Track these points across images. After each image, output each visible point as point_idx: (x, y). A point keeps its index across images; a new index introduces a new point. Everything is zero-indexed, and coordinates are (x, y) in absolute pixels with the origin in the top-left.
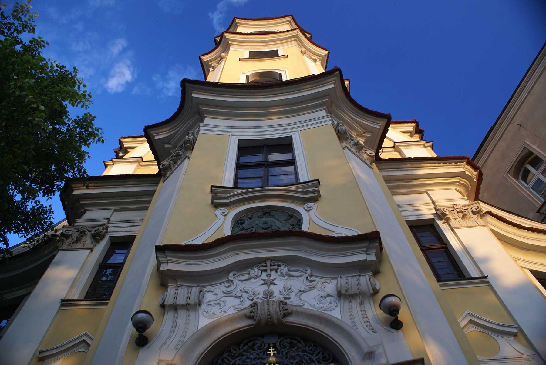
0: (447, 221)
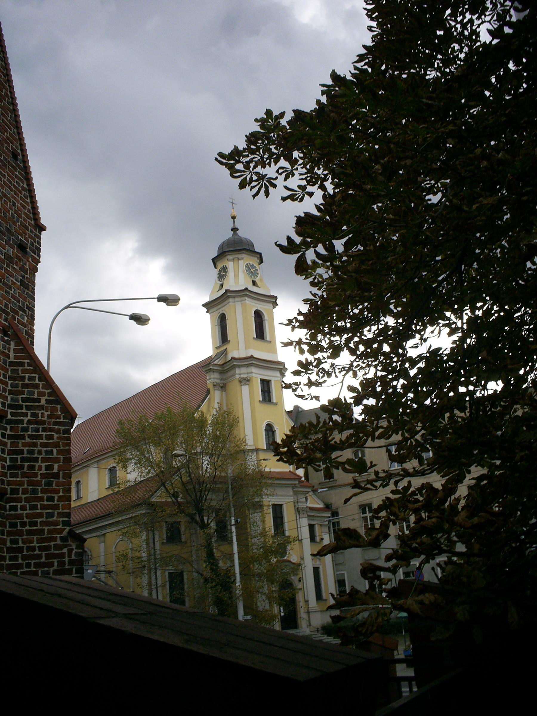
0: (299, 514)
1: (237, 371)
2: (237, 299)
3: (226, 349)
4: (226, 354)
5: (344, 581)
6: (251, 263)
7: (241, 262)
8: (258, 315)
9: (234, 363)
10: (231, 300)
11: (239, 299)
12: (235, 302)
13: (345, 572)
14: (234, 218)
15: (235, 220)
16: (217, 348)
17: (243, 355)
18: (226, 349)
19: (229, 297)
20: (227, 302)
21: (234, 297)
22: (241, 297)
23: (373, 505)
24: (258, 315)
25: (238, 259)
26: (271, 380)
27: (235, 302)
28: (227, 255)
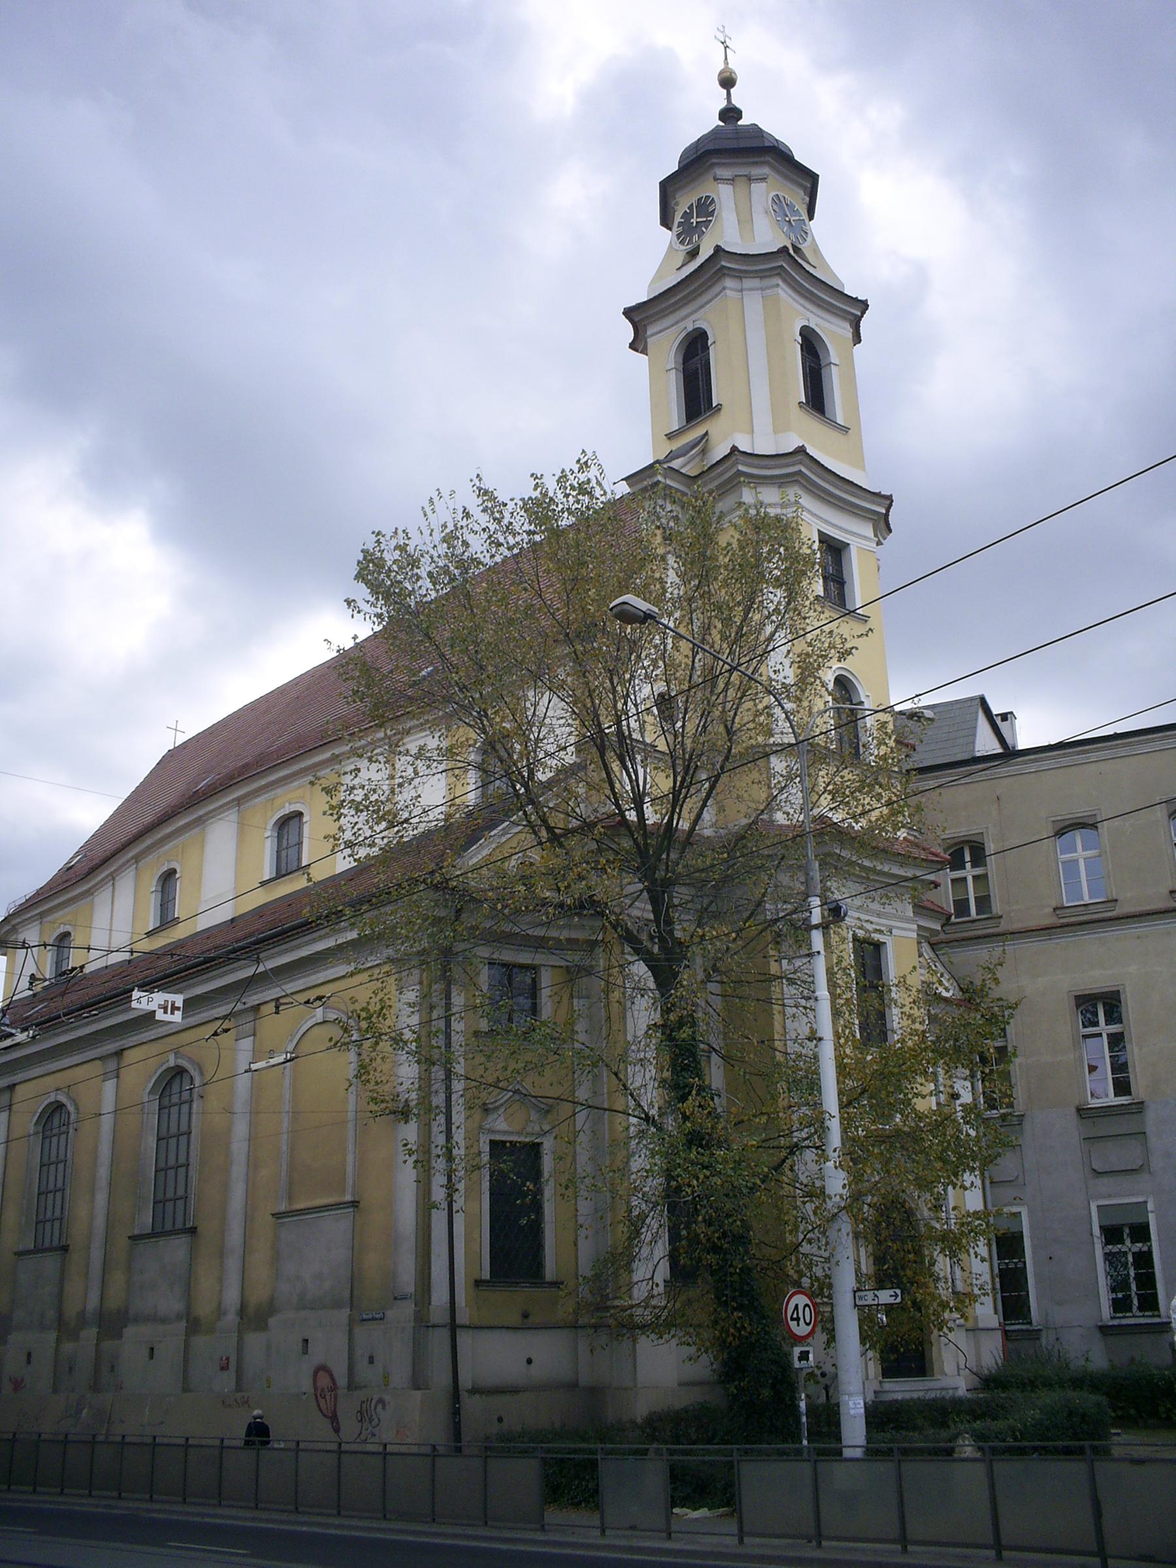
1: (748, 496)
2: (748, 283)
3: (707, 432)
4: (704, 451)
5: (1019, 1237)
6: (789, 199)
7: (758, 188)
8: (811, 345)
9: (741, 468)
10: (729, 283)
11: (756, 283)
12: (741, 290)
13: (1024, 1211)
14: (727, 82)
15: (732, 90)
16: (670, 436)
17: (765, 447)
18: (707, 432)
19: (723, 273)
20: (717, 289)
21: (739, 275)
22: (761, 278)
23: (1122, 997)
24: (811, 345)
25: (750, 179)
26: (848, 544)
27: (741, 290)
28: (713, 165)
